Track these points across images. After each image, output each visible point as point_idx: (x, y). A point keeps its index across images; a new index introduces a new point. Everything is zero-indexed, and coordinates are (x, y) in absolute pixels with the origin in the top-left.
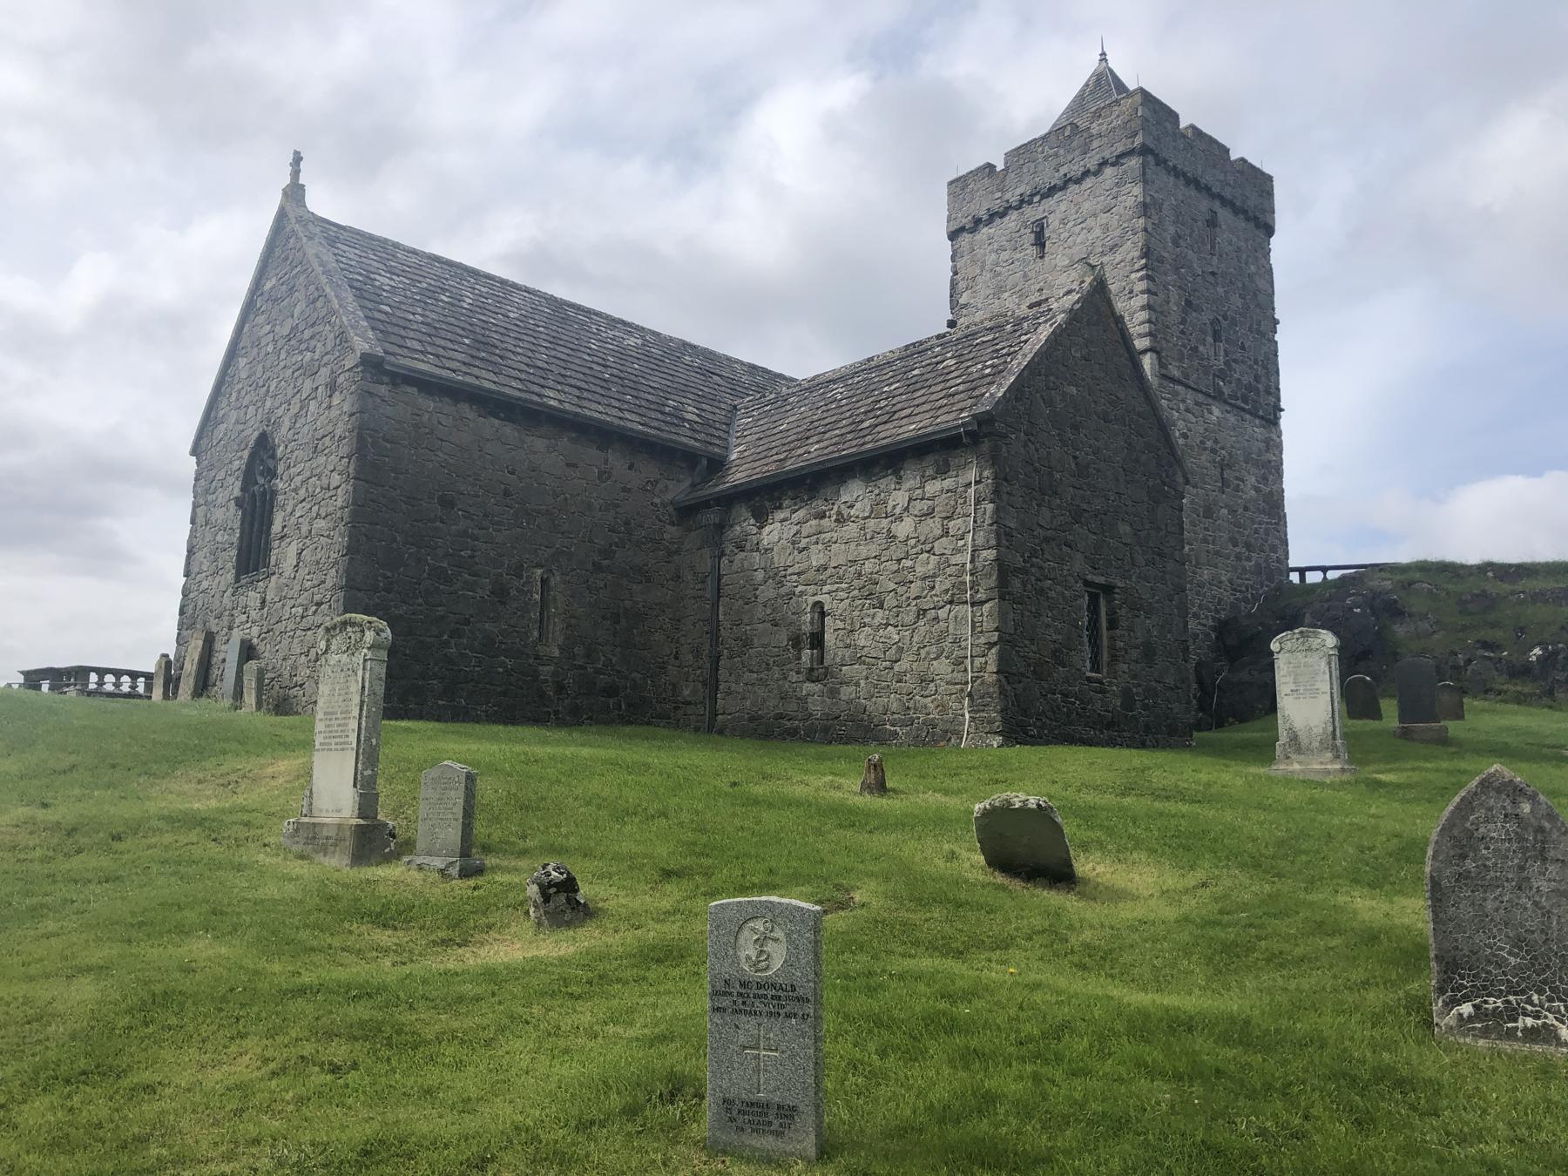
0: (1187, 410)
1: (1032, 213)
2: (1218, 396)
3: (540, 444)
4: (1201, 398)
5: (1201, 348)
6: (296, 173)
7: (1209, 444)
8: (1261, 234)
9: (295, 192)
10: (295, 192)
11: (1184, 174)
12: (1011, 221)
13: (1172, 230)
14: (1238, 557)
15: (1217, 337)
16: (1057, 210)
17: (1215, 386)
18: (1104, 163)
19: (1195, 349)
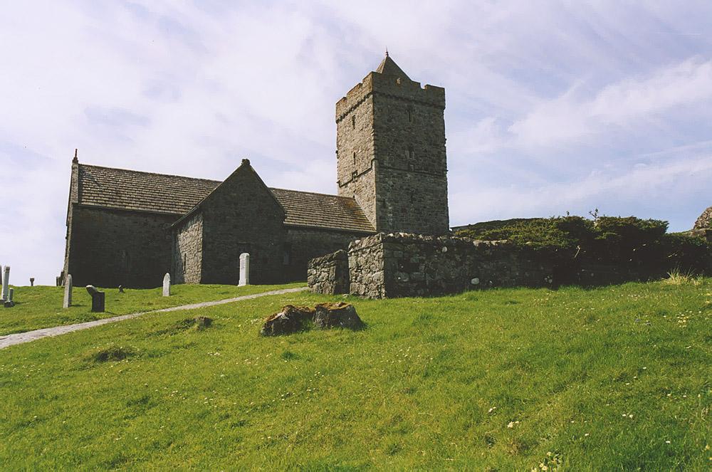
0: (394, 177)
1: (352, 114)
2: (409, 170)
3: (125, 218)
4: (400, 172)
5: (402, 155)
6: (76, 154)
7: (405, 187)
8: (439, 110)
9: (75, 161)
10: (75, 161)
11: (395, 97)
12: (348, 117)
13: (387, 118)
14: (420, 225)
15: (411, 149)
16: (357, 112)
17: (409, 167)
18: (365, 98)
19: (399, 155)
